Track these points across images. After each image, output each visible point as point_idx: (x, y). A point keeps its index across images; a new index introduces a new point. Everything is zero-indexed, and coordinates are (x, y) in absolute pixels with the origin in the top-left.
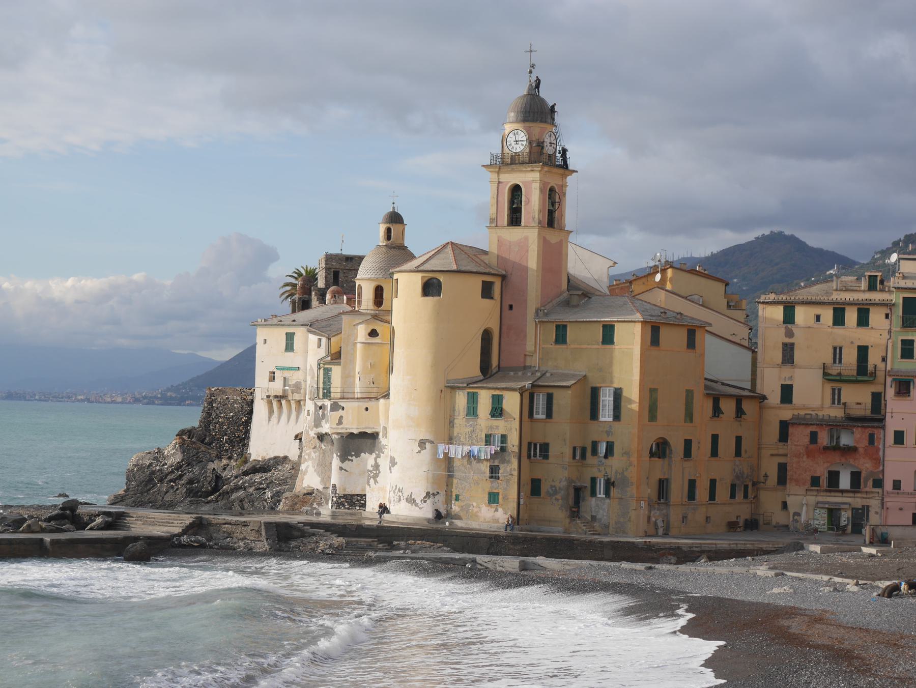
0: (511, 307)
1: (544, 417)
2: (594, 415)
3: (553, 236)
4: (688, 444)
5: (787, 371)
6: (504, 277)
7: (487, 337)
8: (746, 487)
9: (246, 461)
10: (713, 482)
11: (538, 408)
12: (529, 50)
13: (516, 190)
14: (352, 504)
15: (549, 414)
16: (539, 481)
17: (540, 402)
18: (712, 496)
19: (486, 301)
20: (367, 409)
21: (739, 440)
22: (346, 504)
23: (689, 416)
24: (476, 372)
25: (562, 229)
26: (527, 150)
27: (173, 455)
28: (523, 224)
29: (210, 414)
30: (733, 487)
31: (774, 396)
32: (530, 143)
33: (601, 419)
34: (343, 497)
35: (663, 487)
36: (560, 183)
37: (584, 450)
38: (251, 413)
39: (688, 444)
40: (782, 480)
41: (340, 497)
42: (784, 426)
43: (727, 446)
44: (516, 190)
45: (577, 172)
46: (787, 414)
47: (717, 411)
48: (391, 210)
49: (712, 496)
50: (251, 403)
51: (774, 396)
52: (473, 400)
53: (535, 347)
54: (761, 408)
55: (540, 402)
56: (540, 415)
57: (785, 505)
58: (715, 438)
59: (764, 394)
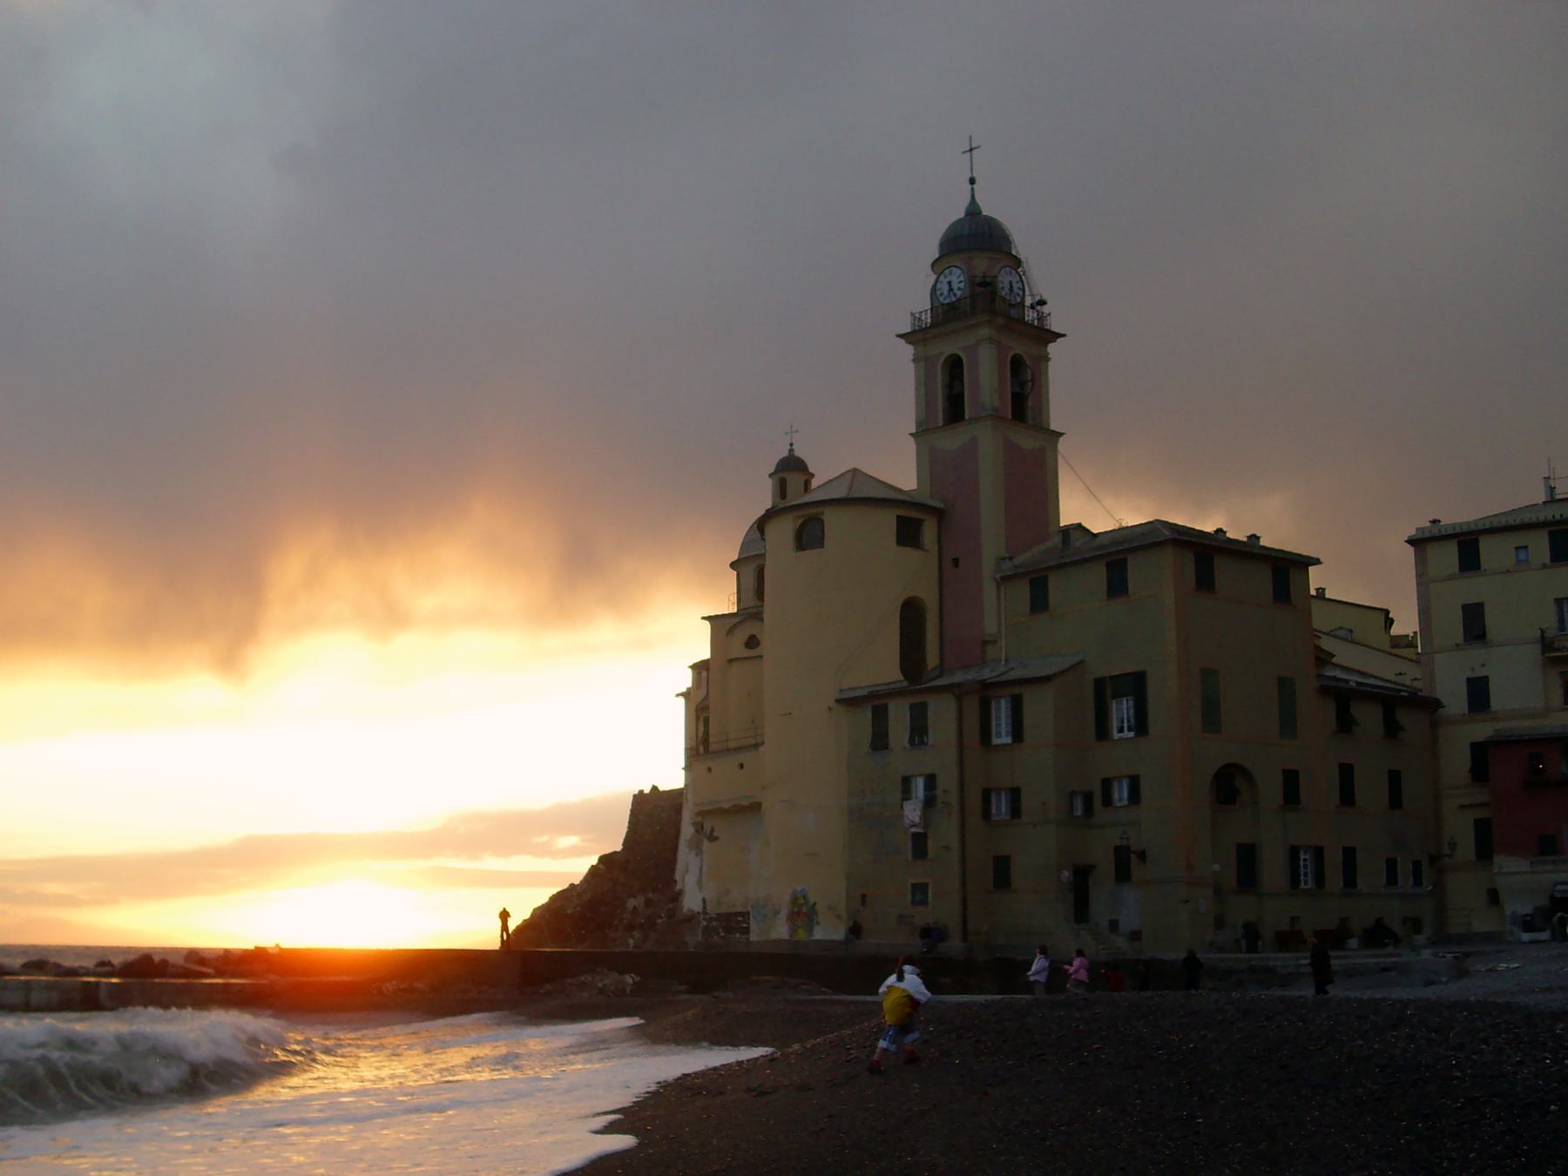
0: (956, 562)
1: (1009, 740)
2: (1102, 732)
3: (1026, 440)
4: (1291, 780)
5: (1477, 654)
6: (939, 514)
7: (911, 613)
10: (1349, 854)
12: (974, 152)
13: (955, 367)
15: (1017, 732)
16: (1007, 859)
17: (1001, 712)
18: (1350, 880)
19: (909, 553)
20: (742, 766)
21: (1395, 778)
22: (720, 930)
30: (1391, 864)
31: (1454, 699)
33: (1116, 735)
34: (716, 920)
35: (1247, 856)
37: (1088, 799)
39: (1291, 780)
40: (1485, 849)
41: (711, 919)
42: (1481, 753)
43: (1372, 789)
44: (955, 367)
45: (1064, 335)
46: (1483, 731)
47: (1345, 724)
48: (785, 454)
49: (1350, 880)
51: (1454, 699)
52: (880, 715)
53: (999, 625)
54: (1434, 725)
55: (1001, 712)
56: (1002, 737)
57: (1493, 897)
58: (1346, 772)
59: (1438, 697)
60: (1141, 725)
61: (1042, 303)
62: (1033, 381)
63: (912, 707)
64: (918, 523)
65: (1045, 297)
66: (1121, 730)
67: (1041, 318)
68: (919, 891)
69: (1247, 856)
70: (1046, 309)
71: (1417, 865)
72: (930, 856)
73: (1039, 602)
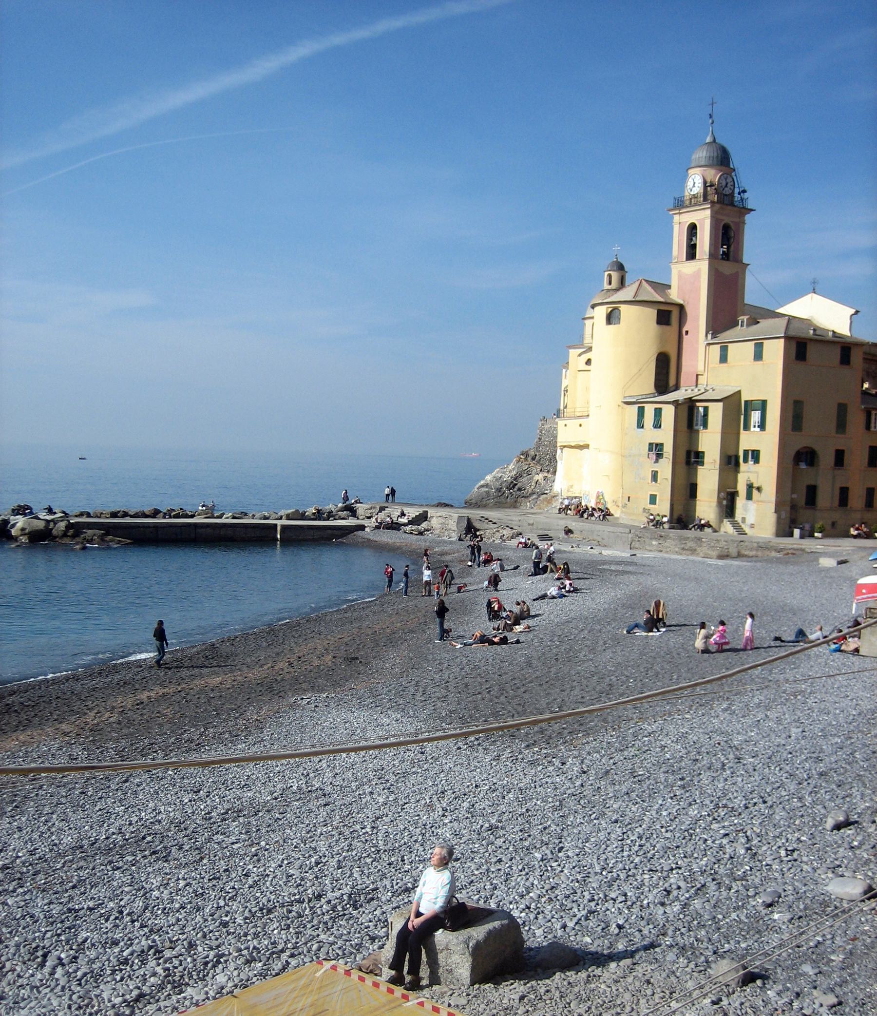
0: (687, 332)
3: (727, 268)
11: (697, 420)
20: (581, 425)
23: (841, 425)
26: (702, 191)
29: (540, 439)
35: (812, 493)
36: (737, 220)
52: (641, 412)
60: (762, 426)
61: (744, 191)
63: (656, 409)
64: (670, 312)
65: (746, 189)
66: (755, 426)
67: (742, 199)
68: (653, 499)
70: (746, 195)
72: (658, 482)
73: (724, 359)
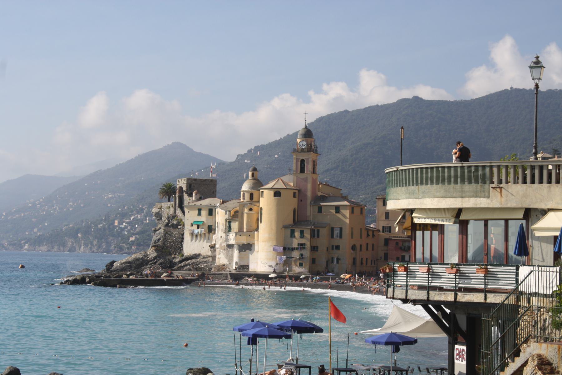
0: (301, 201)
8: (375, 261)
9: (183, 255)
10: (367, 259)
14: (244, 269)
16: (315, 259)
20: (250, 235)
24: (292, 222)
25: (316, 174)
27: (152, 254)
28: (305, 172)
29: (165, 239)
32: (308, 145)
38: (183, 238)
41: (239, 266)
44: (303, 161)
47: (368, 235)
49: (367, 264)
50: (183, 234)
62: (316, 165)
69: (354, 260)
71: (375, 261)
